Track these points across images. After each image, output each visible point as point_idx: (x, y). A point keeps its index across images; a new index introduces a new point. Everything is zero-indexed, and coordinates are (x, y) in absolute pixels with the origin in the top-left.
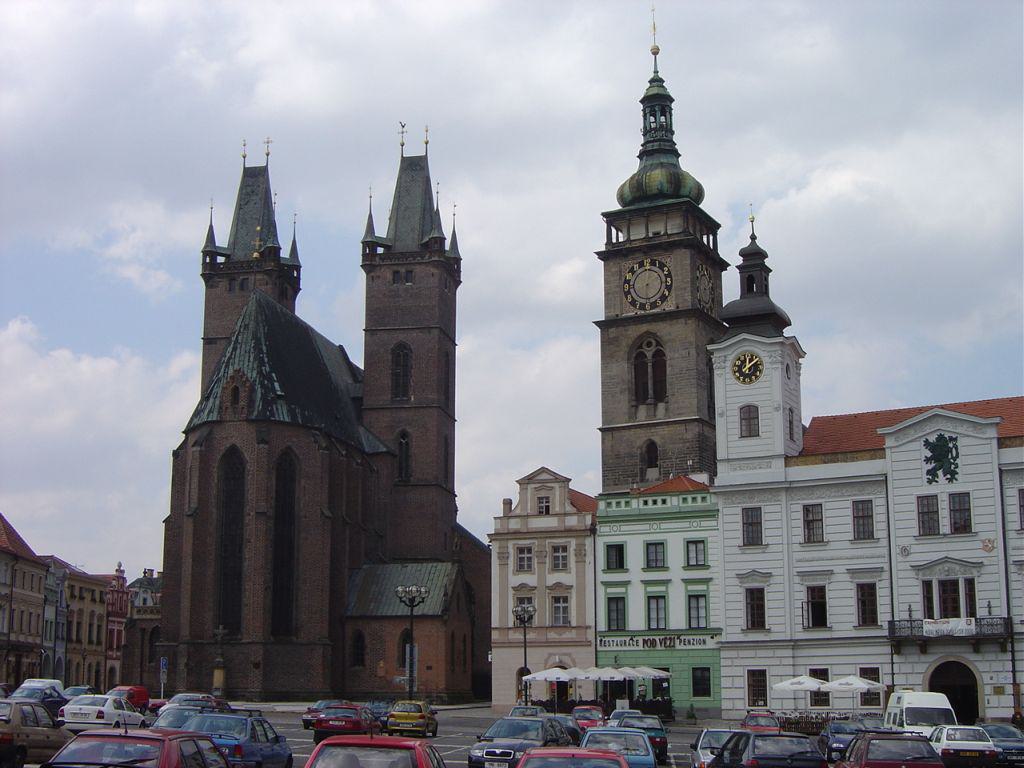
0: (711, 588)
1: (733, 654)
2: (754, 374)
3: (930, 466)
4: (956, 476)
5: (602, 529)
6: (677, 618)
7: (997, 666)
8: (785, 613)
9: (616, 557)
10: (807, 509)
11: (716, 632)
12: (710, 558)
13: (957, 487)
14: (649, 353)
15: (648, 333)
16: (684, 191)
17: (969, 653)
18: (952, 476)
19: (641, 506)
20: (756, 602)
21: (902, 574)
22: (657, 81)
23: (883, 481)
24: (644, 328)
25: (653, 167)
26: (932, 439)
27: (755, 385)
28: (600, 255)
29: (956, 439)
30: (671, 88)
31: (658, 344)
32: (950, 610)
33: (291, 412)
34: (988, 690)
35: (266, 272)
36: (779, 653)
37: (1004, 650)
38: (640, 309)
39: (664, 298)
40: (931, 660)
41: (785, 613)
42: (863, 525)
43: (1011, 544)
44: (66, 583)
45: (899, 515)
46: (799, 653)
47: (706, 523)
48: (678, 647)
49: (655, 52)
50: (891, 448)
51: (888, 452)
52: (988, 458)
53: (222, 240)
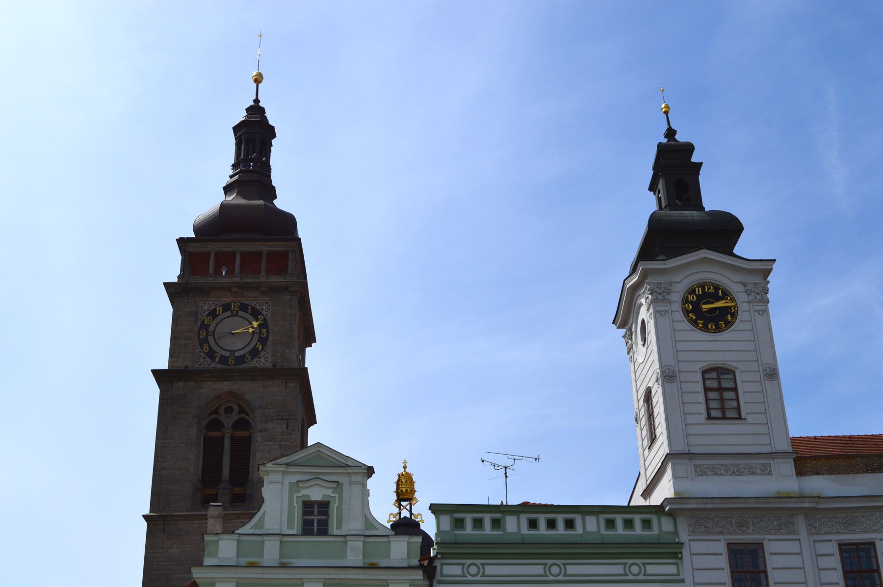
14: (229, 421)
15: (231, 394)
19: (525, 530)
22: (256, 110)
24: (226, 386)
31: (242, 410)
38: (219, 362)
39: (255, 353)
49: (258, 80)
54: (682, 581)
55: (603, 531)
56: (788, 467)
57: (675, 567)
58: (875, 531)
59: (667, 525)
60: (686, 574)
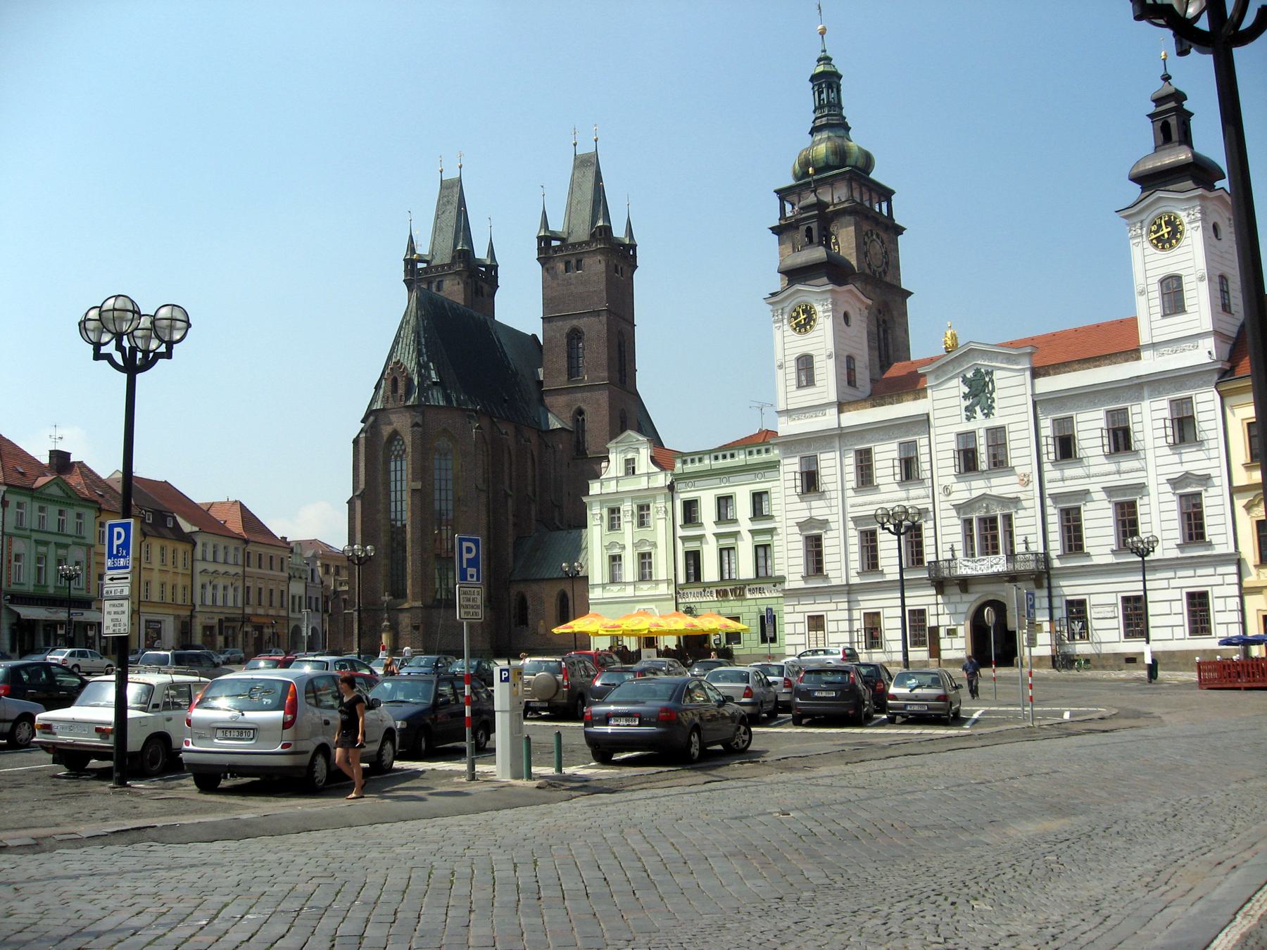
2: (809, 323)
3: (968, 403)
5: (679, 486)
6: (745, 568)
8: (842, 560)
9: (690, 508)
11: (781, 580)
12: (774, 508)
13: (995, 422)
16: (851, 161)
18: (989, 411)
20: (814, 547)
21: (944, 514)
23: (923, 423)
25: (820, 142)
26: (970, 375)
27: (810, 335)
28: (775, 230)
30: (839, 65)
32: (990, 547)
33: (447, 398)
35: (457, 273)
37: (1039, 586)
41: (842, 560)
42: (909, 469)
43: (1047, 476)
44: (319, 563)
45: (939, 455)
46: (853, 597)
48: (748, 596)
50: (931, 387)
51: (929, 391)
52: (1021, 390)
53: (423, 249)
56: (834, 410)
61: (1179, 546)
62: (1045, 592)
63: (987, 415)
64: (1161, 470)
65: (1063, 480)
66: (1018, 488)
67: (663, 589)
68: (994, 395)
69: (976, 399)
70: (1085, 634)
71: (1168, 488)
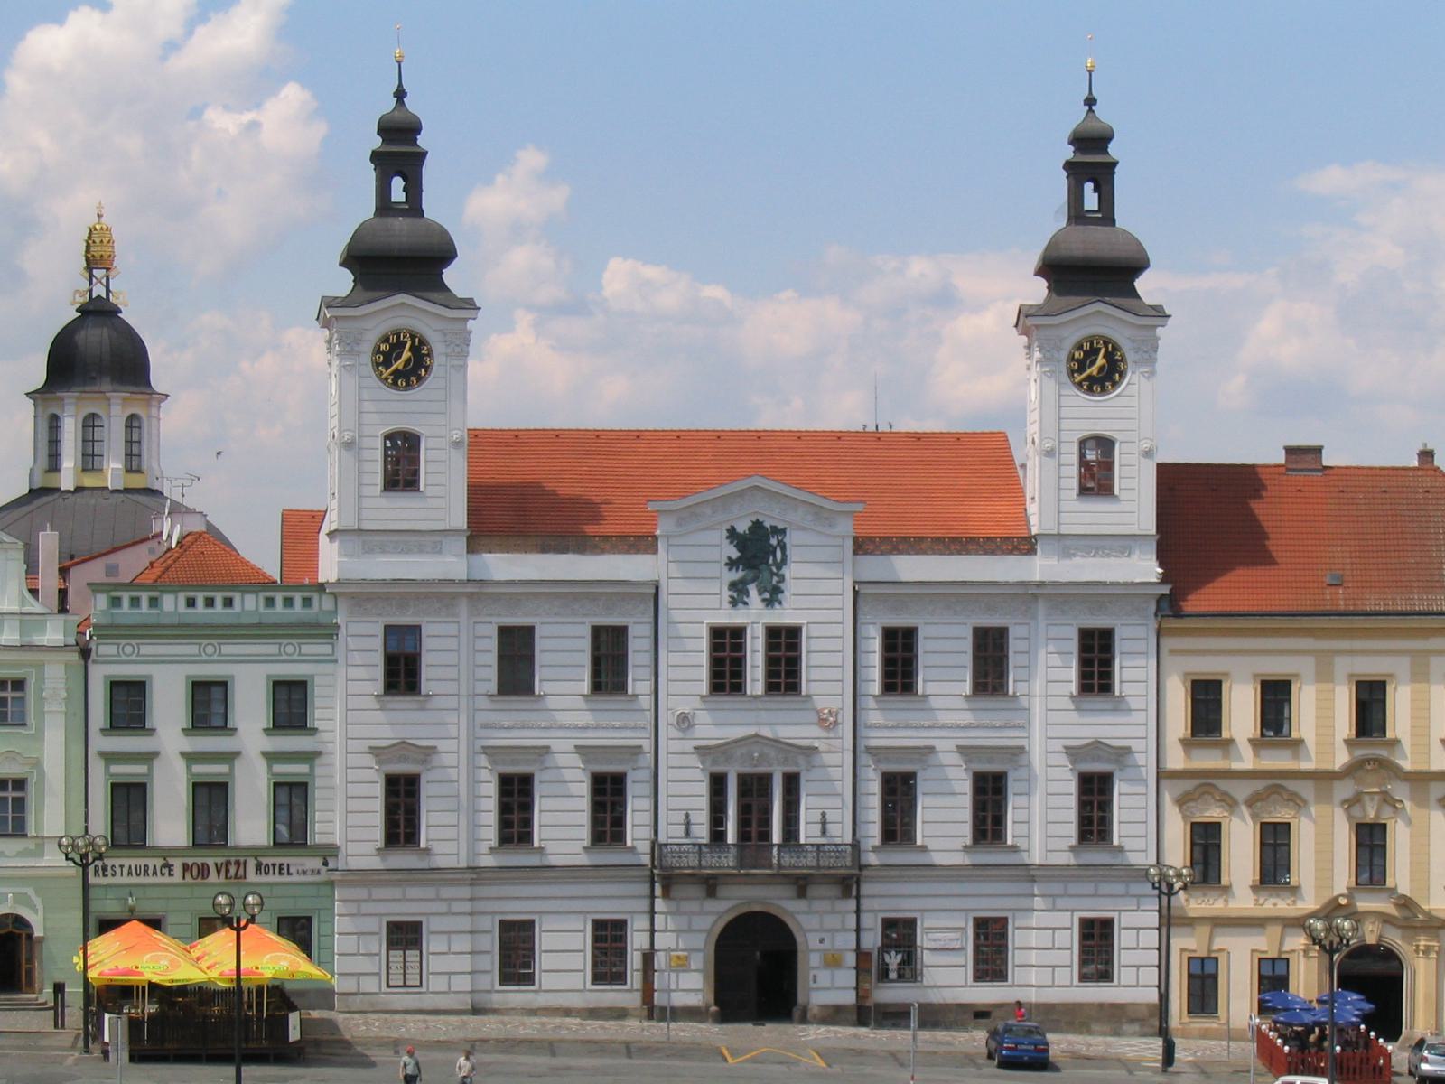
0: (318, 771)
1: (361, 893)
2: (414, 371)
3: (737, 575)
4: (780, 596)
6: (251, 823)
7: (832, 921)
8: (458, 824)
10: (504, 632)
11: (328, 852)
13: (783, 616)
17: (792, 898)
18: (773, 596)
20: (402, 799)
21: (675, 760)
26: (743, 527)
27: (418, 393)
29: (783, 531)
34: (815, 960)
36: (447, 892)
37: (846, 894)
40: (722, 910)
41: (458, 824)
47: (311, 648)
48: (252, 876)
50: (668, 537)
54: (335, 661)
55: (262, 609)
57: (330, 646)
58: (537, 615)
59: (327, 603)
60: (340, 655)
61: (1072, 849)
62: (852, 904)
63: (769, 603)
64: (1053, 732)
65: (892, 728)
66: (815, 731)
67: (54, 859)
68: (785, 571)
69: (751, 574)
70: (910, 969)
71: (1063, 760)
